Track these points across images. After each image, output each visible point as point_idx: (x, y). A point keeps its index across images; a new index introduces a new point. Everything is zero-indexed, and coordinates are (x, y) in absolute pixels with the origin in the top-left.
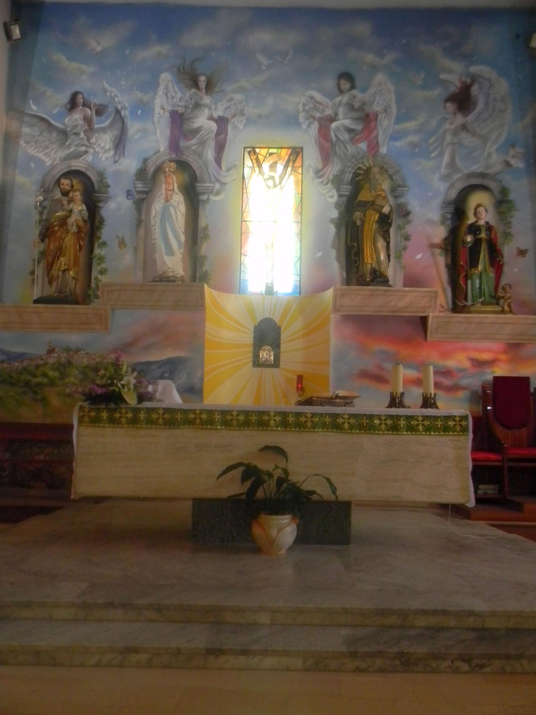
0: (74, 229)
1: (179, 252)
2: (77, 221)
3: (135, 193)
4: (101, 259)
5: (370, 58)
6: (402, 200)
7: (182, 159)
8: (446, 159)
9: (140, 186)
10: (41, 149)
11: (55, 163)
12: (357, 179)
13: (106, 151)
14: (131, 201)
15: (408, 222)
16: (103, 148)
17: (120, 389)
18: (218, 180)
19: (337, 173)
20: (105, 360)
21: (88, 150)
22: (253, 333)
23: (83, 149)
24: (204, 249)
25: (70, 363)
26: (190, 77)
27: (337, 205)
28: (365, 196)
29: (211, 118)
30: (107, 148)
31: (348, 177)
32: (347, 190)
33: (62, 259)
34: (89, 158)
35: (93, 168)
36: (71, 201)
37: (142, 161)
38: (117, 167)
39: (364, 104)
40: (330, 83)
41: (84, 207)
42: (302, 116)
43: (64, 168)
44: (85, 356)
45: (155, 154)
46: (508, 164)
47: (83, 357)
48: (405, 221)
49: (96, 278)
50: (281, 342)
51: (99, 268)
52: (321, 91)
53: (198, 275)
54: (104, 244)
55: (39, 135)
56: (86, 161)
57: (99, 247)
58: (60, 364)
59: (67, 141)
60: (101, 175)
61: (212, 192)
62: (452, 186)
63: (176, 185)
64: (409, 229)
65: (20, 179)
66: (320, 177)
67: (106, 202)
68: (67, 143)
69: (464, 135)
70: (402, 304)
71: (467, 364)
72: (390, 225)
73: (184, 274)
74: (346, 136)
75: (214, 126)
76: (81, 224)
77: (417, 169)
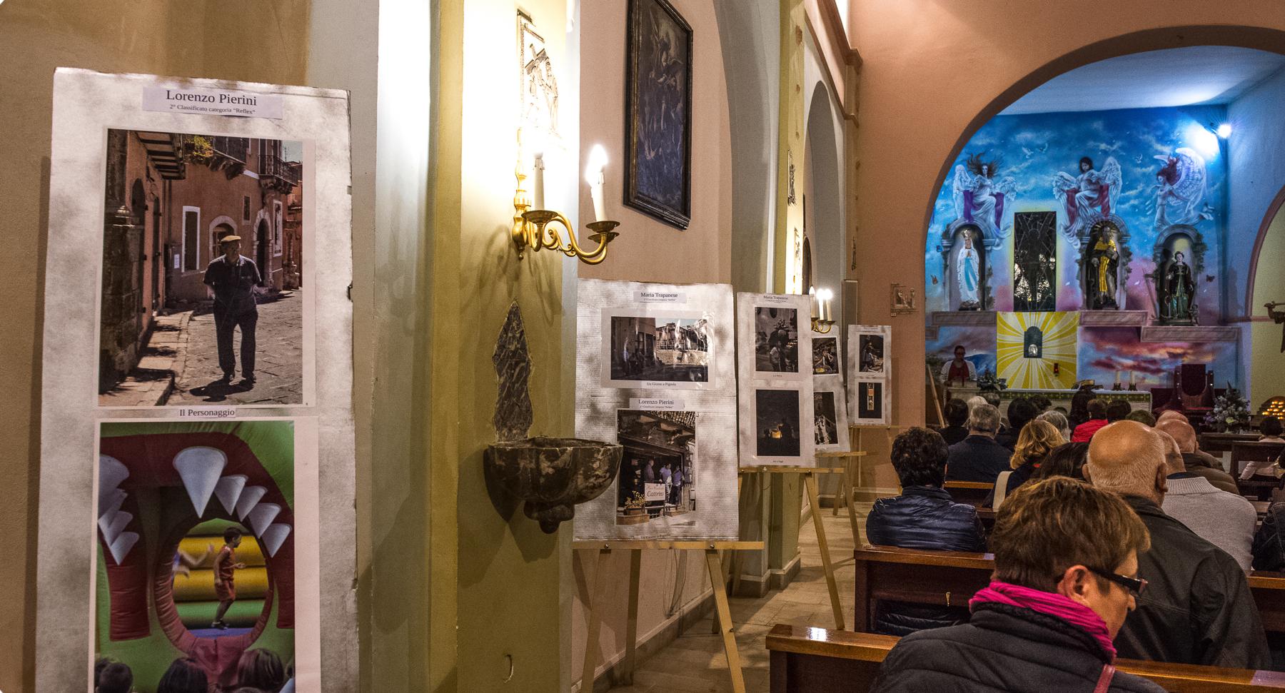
1: (976, 288)
5: (1103, 146)
8: (1158, 216)
24: (989, 283)
26: (975, 167)
27: (1081, 250)
28: (1099, 246)
29: (992, 194)
31: (1088, 231)
32: (1087, 239)
39: (1099, 179)
40: (1075, 166)
42: (1055, 190)
46: (1202, 217)
62: (1161, 234)
64: (1130, 265)
69: (1170, 198)
75: (994, 200)
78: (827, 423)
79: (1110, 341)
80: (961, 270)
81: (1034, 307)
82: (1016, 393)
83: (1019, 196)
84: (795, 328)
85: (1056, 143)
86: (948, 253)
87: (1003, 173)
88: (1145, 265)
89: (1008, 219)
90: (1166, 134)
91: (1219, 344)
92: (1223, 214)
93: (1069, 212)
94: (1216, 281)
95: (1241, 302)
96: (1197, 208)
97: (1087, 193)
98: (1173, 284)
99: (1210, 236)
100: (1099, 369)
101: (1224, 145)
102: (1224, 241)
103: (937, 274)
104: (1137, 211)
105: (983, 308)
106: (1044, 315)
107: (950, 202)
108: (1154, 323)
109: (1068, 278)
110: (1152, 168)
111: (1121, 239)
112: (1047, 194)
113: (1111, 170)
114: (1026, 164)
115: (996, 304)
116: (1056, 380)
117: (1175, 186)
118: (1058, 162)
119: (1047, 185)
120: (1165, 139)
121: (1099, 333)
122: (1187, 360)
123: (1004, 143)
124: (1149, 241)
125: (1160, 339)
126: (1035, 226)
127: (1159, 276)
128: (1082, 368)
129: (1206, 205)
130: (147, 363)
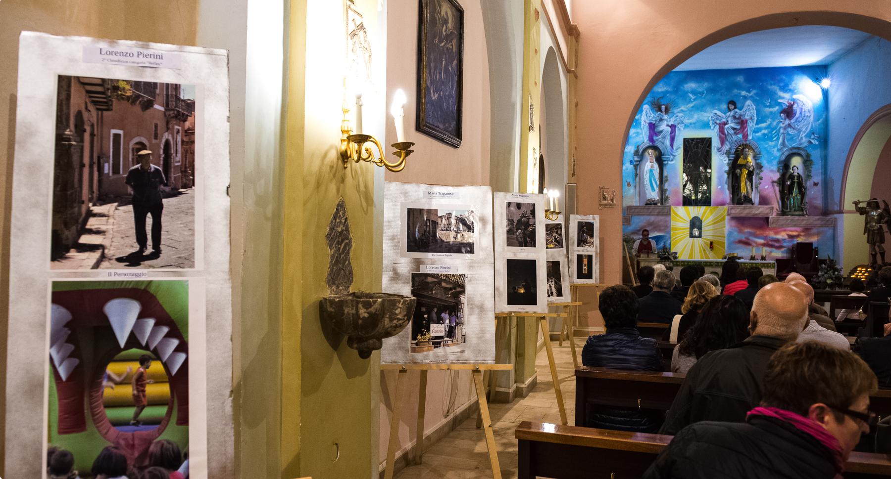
1: (657, 189)
5: (743, 93)
8: (781, 141)
24: (666, 186)
27: (728, 164)
29: (668, 125)
31: (733, 151)
32: (732, 157)
39: (741, 115)
40: (724, 106)
46: (810, 142)
52: (720, 110)
64: (762, 175)
71: (786, 237)
74: (732, 132)
75: (669, 129)
78: (556, 283)
79: (747, 227)
80: (647, 177)
81: (696, 203)
82: (684, 262)
83: (686, 126)
84: (534, 217)
85: (711, 91)
86: (637, 165)
87: (675, 111)
88: (771, 175)
89: (679, 143)
90: (787, 85)
91: (821, 229)
92: (824, 141)
93: (720, 138)
94: (820, 186)
95: (837, 200)
96: (807, 136)
97: (733, 125)
98: (791, 188)
99: (816, 155)
100: (741, 245)
101: (825, 93)
102: (825, 159)
103: (630, 180)
104: (767, 138)
105: (662, 203)
107: (639, 130)
108: (778, 215)
109: (720, 183)
110: (777, 108)
111: (755, 157)
112: (706, 126)
113: (749, 110)
114: (691, 105)
115: (671, 201)
116: (712, 253)
117: (792, 121)
118: (714, 103)
119: (706, 119)
120: (785, 88)
122: (800, 240)
123: (676, 90)
124: (775, 158)
125: (782, 226)
126: (697, 147)
127: (781, 182)
128: (730, 244)
129: (813, 134)
130: (85, 239)
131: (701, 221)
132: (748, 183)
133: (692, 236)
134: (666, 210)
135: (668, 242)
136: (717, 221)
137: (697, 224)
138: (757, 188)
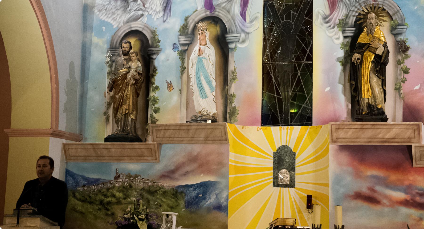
0: (132, 81)
2: (133, 76)
3: (179, 46)
4: (155, 100)
6: (400, 38)
7: (214, 15)
9: (183, 40)
10: (110, 15)
11: (120, 26)
12: (358, 23)
13: (157, 13)
14: (177, 52)
15: (407, 57)
16: (155, 11)
17: (137, 221)
18: (243, 31)
19: (343, 18)
20: (156, 184)
21: (144, 13)
22: (272, 158)
23: (140, 13)
24: (233, 89)
25: (131, 186)
27: (343, 45)
28: (363, 39)
30: (158, 10)
31: (352, 20)
33: (124, 106)
34: (144, 19)
35: (148, 27)
36: (130, 60)
37: (184, 19)
38: (166, 25)
41: (139, 64)
43: (125, 29)
44: (141, 180)
45: (194, 12)
47: (140, 181)
48: (404, 55)
49: (152, 116)
50: (296, 165)
51: (154, 107)
53: (228, 111)
54: (157, 88)
55: (108, 4)
56: (143, 22)
57: (153, 91)
58: (124, 187)
59: (128, 7)
60: (153, 33)
61: (238, 41)
63: (208, 41)
64: (407, 63)
65: (95, 40)
66: (327, 22)
67: (158, 54)
68: (128, 9)
70: (389, 136)
72: (385, 63)
73: (216, 112)
76: (138, 77)
77: (416, 8)
80: (192, 71)
81: (288, 121)
103: (173, 78)
106: (297, 130)
111: (395, 30)
115: (241, 115)
121: (358, 153)
126: (288, 17)
131: (293, 155)
132: (375, 80)
133: (276, 184)
134: (218, 133)
135: (224, 195)
136: (320, 156)
137: (288, 160)
138: (398, 89)
